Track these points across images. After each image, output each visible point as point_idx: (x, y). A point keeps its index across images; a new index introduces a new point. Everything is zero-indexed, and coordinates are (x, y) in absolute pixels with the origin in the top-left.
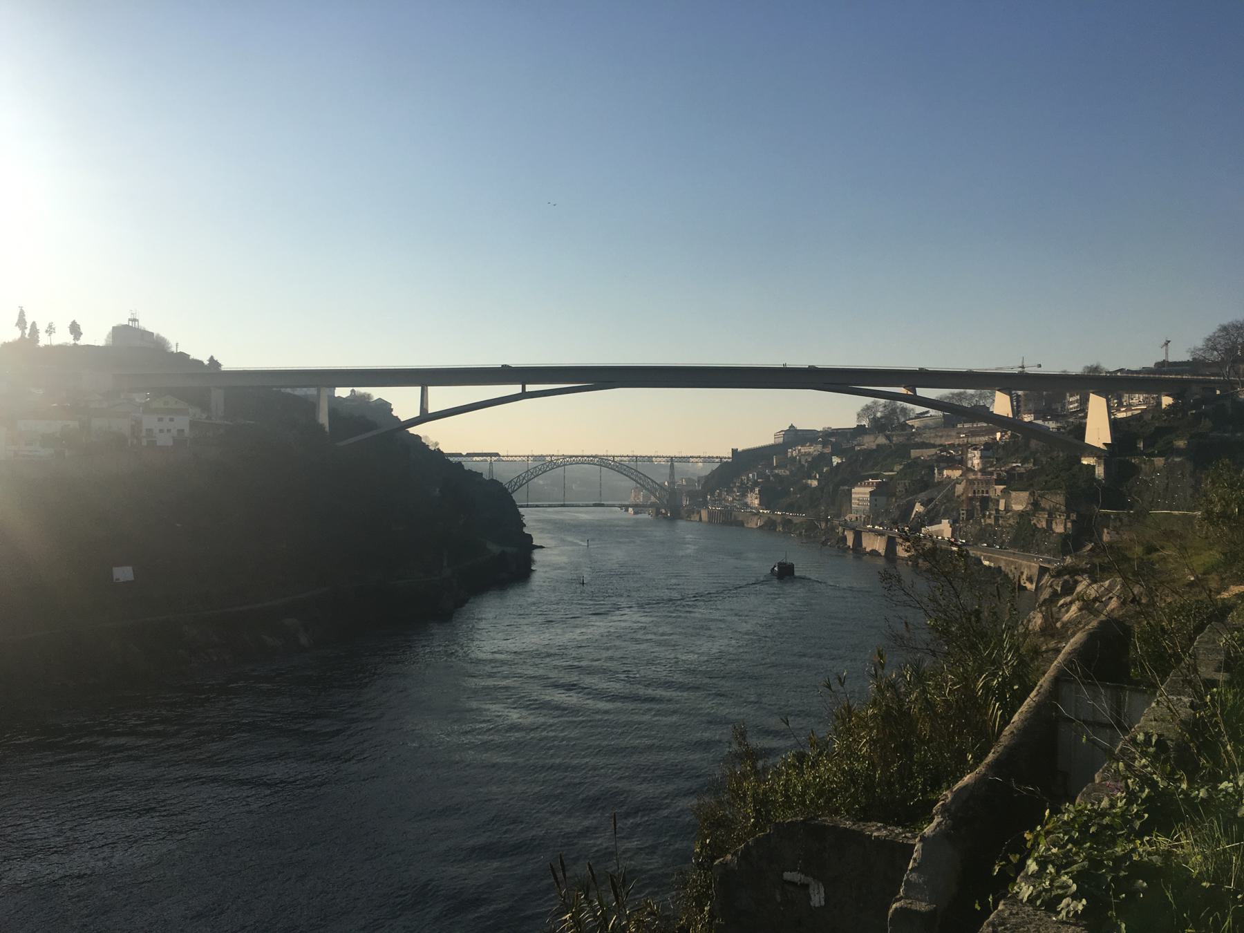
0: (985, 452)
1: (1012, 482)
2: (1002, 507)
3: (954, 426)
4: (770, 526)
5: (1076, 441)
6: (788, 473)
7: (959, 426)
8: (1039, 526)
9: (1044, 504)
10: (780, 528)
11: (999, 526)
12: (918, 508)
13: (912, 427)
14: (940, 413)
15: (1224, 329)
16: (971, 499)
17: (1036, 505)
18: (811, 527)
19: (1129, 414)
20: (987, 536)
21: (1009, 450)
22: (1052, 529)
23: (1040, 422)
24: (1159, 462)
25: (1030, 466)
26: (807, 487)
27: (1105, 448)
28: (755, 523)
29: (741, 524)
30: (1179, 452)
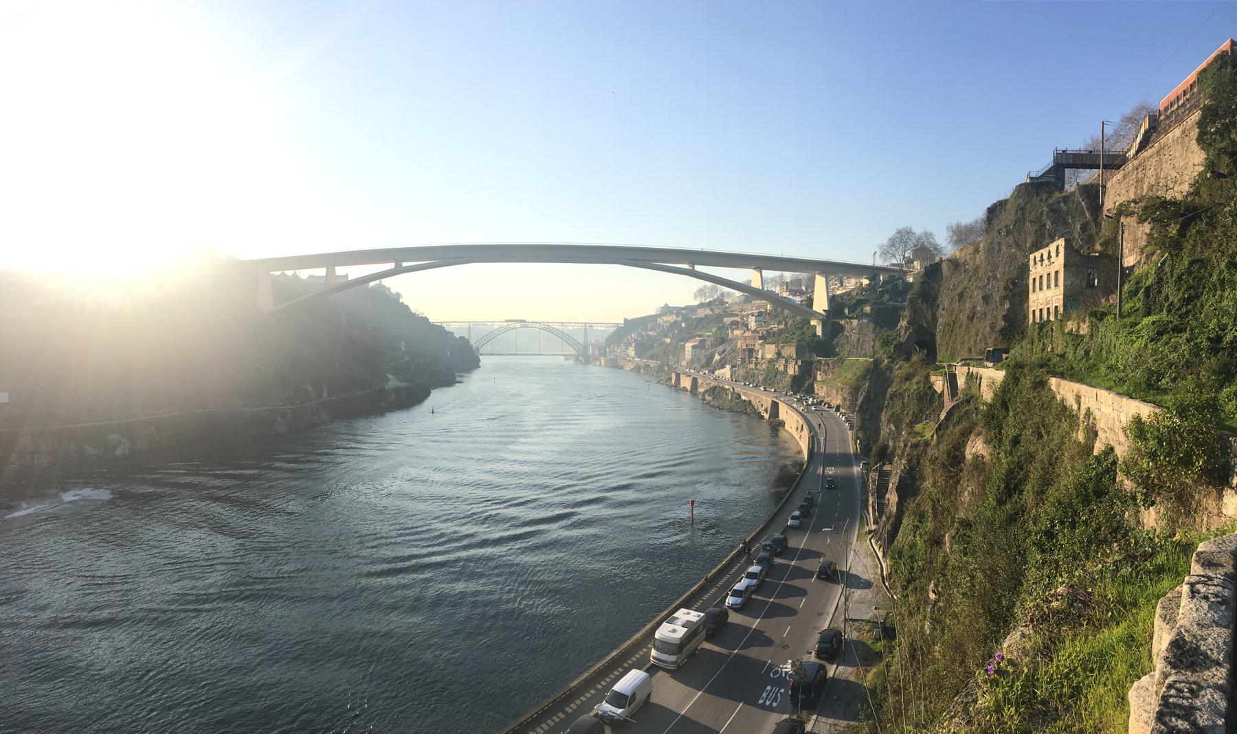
0: (758, 318)
1: (766, 338)
2: (760, 356)
3: (751, 302)
4: (637, 369)
5: (809, 309)
6: (656, 334)
7: (753, 302)
8: (780, 370)
9: (784, 353)
10: (642, 371)
11: (757, 369)
12: (717, 357)
13: (727, 303)
14: (742, 294)
15: (900, 232)
16: (744, 350)
17: (779, 354)
18: (660, 369)
19: (844, 291)
20: (749, 378)
21: (773, 315)
22: (787, 372)
23: (791, 297)
24: (855, 322)
25: (782, 326)
26: (664, 342)
27: (824, 313)
28: (630, 366)
29: (622, 368)
30: (867, 315)
